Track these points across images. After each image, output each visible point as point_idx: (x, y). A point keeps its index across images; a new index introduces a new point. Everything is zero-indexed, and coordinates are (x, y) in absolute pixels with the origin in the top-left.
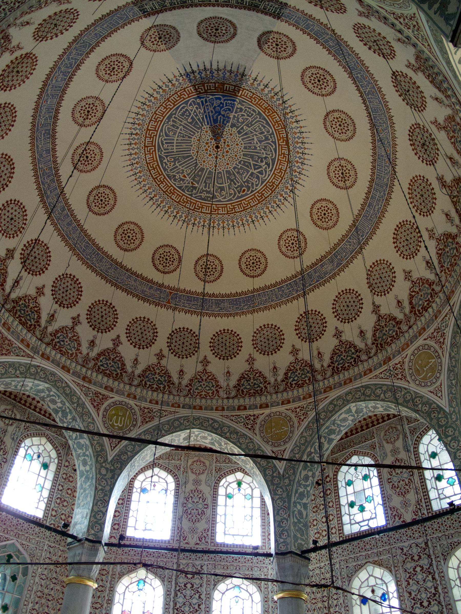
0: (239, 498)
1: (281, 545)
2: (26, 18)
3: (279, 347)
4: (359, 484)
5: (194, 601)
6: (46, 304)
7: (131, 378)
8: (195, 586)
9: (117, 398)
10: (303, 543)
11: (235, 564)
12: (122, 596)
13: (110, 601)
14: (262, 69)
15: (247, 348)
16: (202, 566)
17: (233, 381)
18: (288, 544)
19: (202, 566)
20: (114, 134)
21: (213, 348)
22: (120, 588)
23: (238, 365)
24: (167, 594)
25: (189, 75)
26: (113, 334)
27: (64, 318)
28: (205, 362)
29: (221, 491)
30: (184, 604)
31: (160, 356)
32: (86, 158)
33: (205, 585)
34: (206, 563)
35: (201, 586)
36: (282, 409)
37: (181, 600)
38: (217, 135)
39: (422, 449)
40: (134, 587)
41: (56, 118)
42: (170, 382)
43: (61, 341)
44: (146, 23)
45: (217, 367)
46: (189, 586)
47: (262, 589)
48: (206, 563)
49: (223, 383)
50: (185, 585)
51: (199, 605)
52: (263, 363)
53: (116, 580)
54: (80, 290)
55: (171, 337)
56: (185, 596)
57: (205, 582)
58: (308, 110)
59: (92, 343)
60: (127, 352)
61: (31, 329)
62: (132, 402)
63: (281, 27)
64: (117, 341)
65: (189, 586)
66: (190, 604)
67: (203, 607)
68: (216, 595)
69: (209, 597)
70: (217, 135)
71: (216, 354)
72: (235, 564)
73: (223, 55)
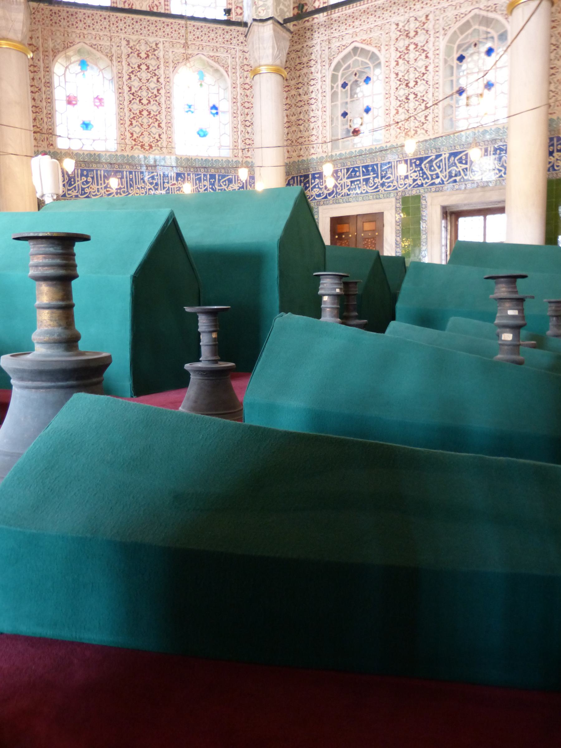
1: (260, 9)
5: (152, 85)
8: (151, 68)
10: (286, 10)
11: (198, 43)
12: (62, 78)
13: (49, 84)
16: (157, 44)
18: (268, 8)
19: (157, 44)
22: (58, 68)
30: (140, 88)
33: (162, 66)
35: (158, 68)
37: (136, 84)
40: (75, 68)
46: (144, 67)
47: (230, 74)
48: (161, 40)
50: (139, 67)
51: (158, 90)
53: (51, 58)
56: (140, 80)
57: (162, 63)
65: (144, 67)
66: (148, 89)
67: (162, 92)
72: (198, 43)
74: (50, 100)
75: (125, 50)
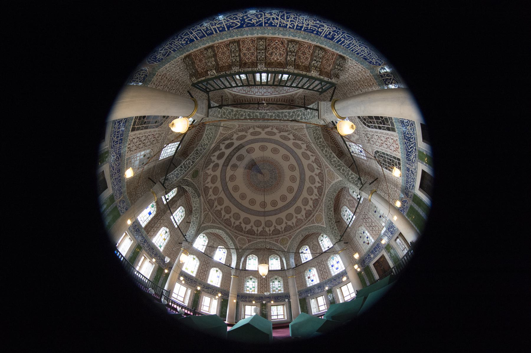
0: (324, 240)
2: (206, 182)
3: (308, 202)
4: (346, 214)
6: (255, 228)
7: (282, 232)
9: (281, 238)
13: (304, 277)
14: (257, 155)
15: (303, 207)
17: (304, 216)
20: (244, 188)
21: (296, 213)
23: (303, 212)
24: (317, 269)
25: (245, 168)
26: (273, 226)
27: (260, 229)
28: (296, 217)
29: (319, 241)
31: (286, 223)
32: (243, 196)
34: (323, 257)
36: (317, 213)
38: (261, 173)
39: (351, 193)
41: (231, 194)
42: (291, 227)
43: (263, 234)
44: (229, 167)
45: (299, 216)
49: (302, 218)
52: (308, 208)
54: (261, 222)
55: (286, 218)
58: (268, 154)
59: (270, 230)
60: (278, 227)
61: (254, 235)
62: (285, 237)
63: (247, 147)
64: (275, 227)
68: (328, 262)
69: (327, 264)
70: (261, 173)
71: (298, 214)
73: (246, 161)
74: (305, 279)
75: (316, 264)
